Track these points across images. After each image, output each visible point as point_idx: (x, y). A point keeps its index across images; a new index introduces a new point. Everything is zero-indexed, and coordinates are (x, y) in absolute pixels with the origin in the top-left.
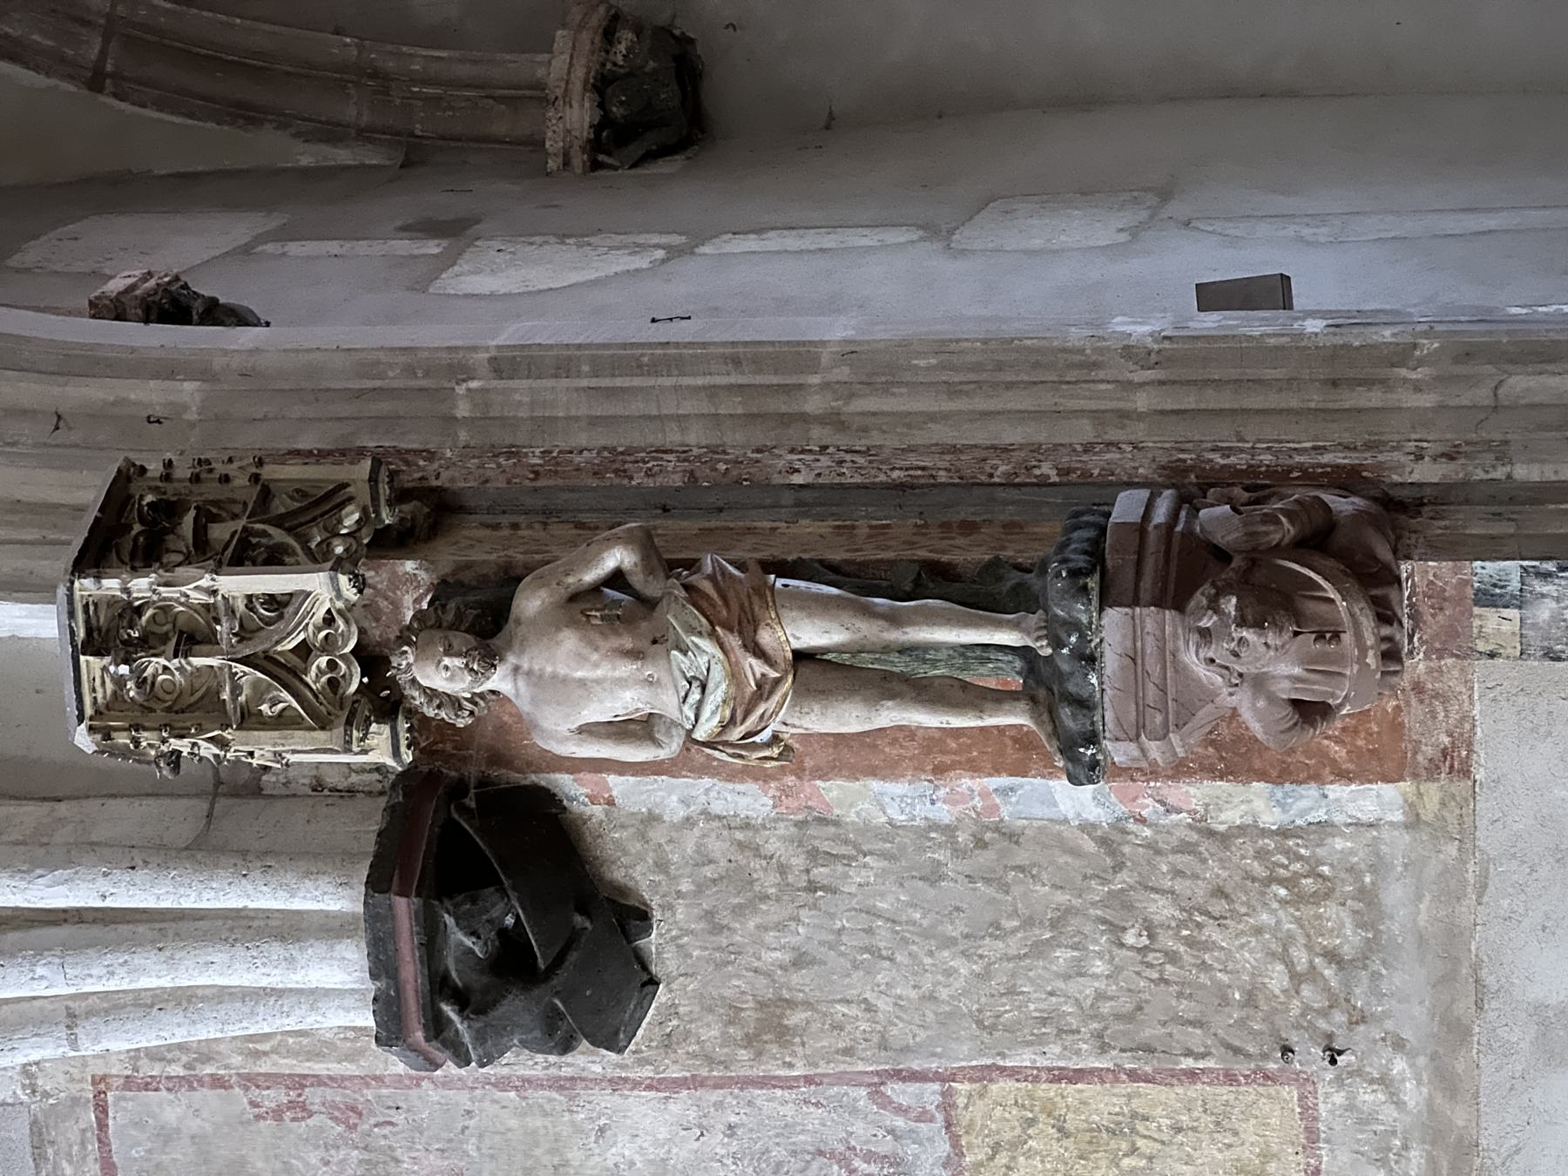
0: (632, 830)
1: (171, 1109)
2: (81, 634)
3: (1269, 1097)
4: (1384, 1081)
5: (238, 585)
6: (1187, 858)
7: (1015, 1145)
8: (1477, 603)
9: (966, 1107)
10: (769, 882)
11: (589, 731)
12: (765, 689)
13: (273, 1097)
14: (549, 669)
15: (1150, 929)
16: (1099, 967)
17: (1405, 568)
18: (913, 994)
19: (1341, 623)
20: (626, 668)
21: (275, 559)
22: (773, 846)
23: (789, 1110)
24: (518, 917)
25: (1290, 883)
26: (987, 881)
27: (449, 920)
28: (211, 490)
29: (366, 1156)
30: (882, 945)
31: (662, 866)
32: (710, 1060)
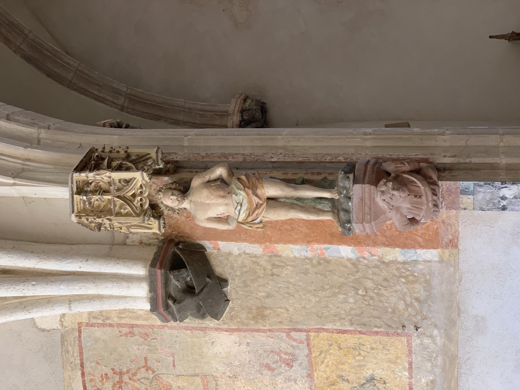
0: (224, 257)
1: (98, 332)
2: (75, 190)
3: (399, 340)
4: (431, 337)
5: (117, 176)
6: (377, 269)
7: (327, 351)
8: (461, 193)
9: (313, 340)
10: (261, 273)
11: (210, 219)
12: (258, 206)
13: (125, 330)
14: (199, 200)
15: (366, 290)
16: (351, 300)
17: (440, 183)
18: (299, 306)
19: (422, 193)
20: (221, 201)
21: (128, 169)
22: (262, 262)
23: (264, 339)
24: (191, 278)
25: (406, 277)
26: (321, 274)
27: (172, 277)
28: (113, 155)
29: (149, 348)
30: (291, 292)
31: (232, 268)
32: (243, 324)
